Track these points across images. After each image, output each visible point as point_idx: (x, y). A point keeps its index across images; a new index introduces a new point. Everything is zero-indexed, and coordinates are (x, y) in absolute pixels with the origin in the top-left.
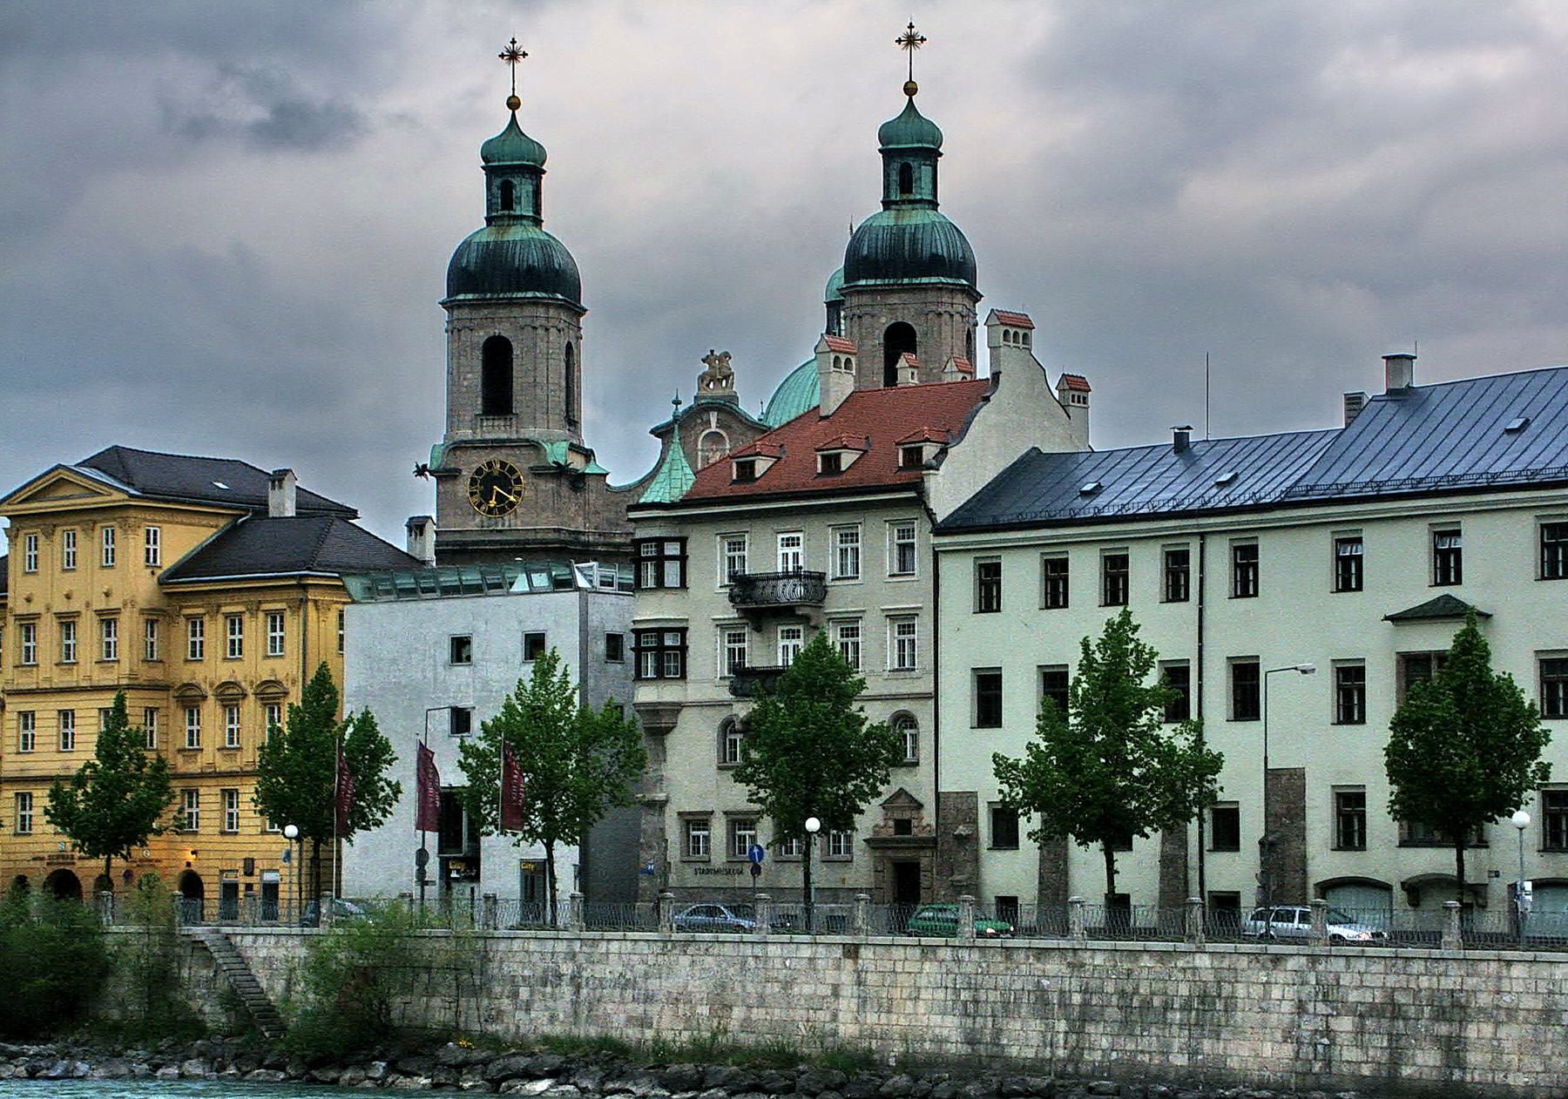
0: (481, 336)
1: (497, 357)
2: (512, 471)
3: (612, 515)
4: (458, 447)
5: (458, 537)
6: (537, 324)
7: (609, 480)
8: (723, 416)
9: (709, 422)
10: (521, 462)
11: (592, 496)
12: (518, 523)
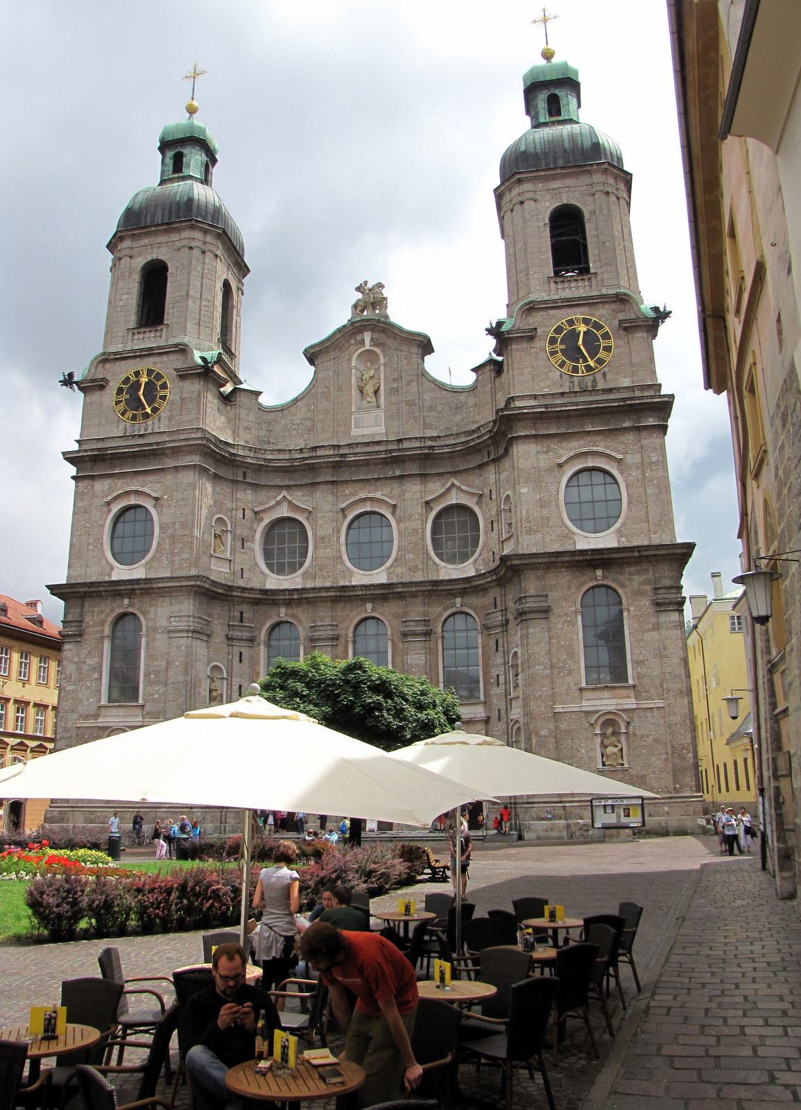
0: (140, 262)
1: (154, 280)
2: (159, 376)
3: (263, 433)
4: (106, 359)
5: (100, 445)
6: (193, 244)
7: (263, 400)
8: (376, 335)
9: (362, 342)
10: (167, 367)
11: (243, 412)
12: (161, 425)
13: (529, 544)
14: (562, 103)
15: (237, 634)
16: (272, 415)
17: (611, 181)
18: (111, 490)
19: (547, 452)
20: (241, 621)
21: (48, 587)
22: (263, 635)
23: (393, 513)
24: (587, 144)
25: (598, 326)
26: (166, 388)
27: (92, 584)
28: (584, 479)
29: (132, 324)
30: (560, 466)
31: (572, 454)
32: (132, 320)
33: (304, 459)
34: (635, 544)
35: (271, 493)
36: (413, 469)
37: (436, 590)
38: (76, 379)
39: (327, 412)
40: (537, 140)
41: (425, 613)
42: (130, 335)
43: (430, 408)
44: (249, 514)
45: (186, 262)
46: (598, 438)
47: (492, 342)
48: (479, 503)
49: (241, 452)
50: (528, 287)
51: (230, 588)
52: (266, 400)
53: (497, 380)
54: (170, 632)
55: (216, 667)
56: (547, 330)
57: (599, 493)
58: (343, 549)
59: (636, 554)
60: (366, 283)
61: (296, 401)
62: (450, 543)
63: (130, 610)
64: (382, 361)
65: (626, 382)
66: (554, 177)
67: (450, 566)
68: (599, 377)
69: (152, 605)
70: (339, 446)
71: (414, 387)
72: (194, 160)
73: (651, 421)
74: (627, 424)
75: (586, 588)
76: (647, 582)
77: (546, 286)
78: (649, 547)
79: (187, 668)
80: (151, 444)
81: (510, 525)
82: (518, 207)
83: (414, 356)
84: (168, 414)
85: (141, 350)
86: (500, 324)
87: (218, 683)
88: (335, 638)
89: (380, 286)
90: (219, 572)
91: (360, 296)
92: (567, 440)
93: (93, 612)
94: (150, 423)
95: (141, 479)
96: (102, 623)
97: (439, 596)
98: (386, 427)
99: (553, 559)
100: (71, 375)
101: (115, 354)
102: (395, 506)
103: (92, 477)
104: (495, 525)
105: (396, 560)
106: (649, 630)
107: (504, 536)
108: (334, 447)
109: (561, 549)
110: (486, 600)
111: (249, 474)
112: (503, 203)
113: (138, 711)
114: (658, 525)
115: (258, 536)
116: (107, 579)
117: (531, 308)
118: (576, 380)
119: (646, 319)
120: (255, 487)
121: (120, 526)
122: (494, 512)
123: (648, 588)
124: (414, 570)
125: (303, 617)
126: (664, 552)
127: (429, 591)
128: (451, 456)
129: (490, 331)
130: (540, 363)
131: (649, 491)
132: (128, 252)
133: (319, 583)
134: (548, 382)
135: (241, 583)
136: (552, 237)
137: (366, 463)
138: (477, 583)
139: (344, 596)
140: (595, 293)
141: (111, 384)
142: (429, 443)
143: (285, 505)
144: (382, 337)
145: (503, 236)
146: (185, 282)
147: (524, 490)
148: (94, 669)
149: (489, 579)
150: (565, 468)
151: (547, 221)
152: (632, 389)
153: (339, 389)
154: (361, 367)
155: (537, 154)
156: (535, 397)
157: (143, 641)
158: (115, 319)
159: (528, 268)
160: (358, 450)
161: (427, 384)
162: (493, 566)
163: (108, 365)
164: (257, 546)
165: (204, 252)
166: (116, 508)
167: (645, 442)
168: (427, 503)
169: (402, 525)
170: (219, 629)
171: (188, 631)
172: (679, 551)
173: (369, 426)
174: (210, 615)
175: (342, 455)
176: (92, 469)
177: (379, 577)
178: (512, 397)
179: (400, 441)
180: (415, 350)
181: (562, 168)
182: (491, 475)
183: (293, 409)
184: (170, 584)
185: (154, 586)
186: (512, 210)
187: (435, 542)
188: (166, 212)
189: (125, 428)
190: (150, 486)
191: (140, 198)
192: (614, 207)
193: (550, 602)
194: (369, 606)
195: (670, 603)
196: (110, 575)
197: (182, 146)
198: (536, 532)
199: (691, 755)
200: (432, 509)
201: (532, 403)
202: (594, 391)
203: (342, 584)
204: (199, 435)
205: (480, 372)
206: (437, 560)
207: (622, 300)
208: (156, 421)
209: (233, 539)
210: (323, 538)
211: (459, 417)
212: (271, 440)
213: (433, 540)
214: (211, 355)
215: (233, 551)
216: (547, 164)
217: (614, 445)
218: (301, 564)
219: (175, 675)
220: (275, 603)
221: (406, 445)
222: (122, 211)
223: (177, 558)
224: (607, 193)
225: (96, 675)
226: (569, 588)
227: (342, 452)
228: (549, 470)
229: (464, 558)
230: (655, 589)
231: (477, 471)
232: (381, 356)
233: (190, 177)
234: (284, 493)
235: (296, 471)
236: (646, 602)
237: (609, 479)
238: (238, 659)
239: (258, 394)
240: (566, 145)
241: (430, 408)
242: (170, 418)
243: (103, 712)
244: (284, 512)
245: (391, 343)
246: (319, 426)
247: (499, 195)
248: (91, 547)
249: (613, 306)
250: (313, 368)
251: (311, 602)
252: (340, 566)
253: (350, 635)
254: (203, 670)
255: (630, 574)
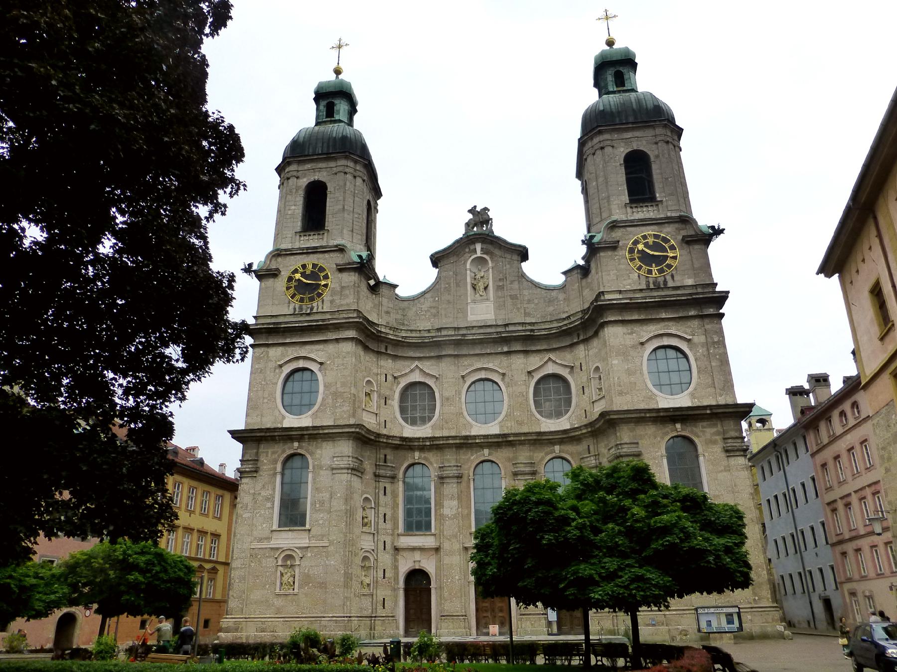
0: (304, 182)
2: (322, 269)
3: (399, 317)
4: (277, 254)
5: (273, 320)
6: (347, 170)
8: (485, 246)
9: (475, 251)
11: (385, 301)
12: (325, 306)
13: (621, 403)
14: (626, 77)
15: (382, 472)
16: (406, 303)
17: (669, 134)
18: (283, 355)
19: (631, 333)
20: (385, 462)
21: (229, 431)
22: (401, 475)
23: (503, 380)
24: (650, 105)
25: (666, 240)
26: (328, 278)
27: (268, 430)
28: (661, 353)
29: (299, 229)
30: (642, 344)
31: (652, 335)
32: (298, 225)
33: (433, 337)
34: (705, 403)
35: (407, 363)
36: (517, 347)
37: (540, 440)
38: (255, 267)
39: (449, 302)
40: (612, 103)
41: (531, 458)
42: (298, 237)
43: (529, 301)
44: (390, 378)
45: (341, 183)
46: (670, 324)
47: (583, 249)
48: (570, 373)
49: (383, 330)
50: (610, 210)
51: (379, 435)
52: (401, 292)
53: (584, 280)
54: (333, 469)
55: (366, 499)
56: (626, 242)
57: (673, 364)
58: (464, 406)
59: (708, 412)
60: (475, 207)
61: (424, 293)
62: (548, 404)
63: (299, 451)
64: (490, 264)
65: (690, 282)
66: (627, 130)
67: (548, 421)
68: (668, 278)
69: (317, 448)
70: (459, 328)
71: (516, 285)
72: (342, 107)
73: (711, 311)
74: (692, 313)
75: (669, 437)
76: (718, 433)
77: (624, 210)
78: (718, 406)
79: (348, 499)
80: (317, 321)
81: (600, 389)
82: (599, 152)
83: (516, 262)
84: (330, 298)
85: (308, 248)
86: (592, 237)
87: (368, 511)
88: (459, 477)
89: (486, 209)
90: (370, 422)
91: (471, 216)
92: (647, 324)
93: (267, 452)
94: (315, 304)
95: (308, 347)
96: (275, 462)
97: (542, 444)
98: (496, 315)
99: (643, 415)
100: (250, 265)
101: (286, 250)
102: (504, 375)
103: (267, 345)
104: (586, 390)
105: (506, 416)
106: (721, 471)
107: (594, 399)
108: (455, 328)
109: (647, 407)
110: (581, 448)
111: (390, 347)
112: (585, 149)
113: (306, 535)
114: (723, 389)
115: (397, 396)
116: (279, 426)
117: (614, 226)
118: (651, 280)
119: (704, 234)
120: (395, 357)
121: (289, 384)
122: (585, 379)
123: (718, 438)
124: (520, 423)
125: (433, 460)
126: (731, 410)
127: (535, 440)
128: (547, 338)
129: (583, 242)
130: (622, 267)
131: (713, 364)
132: (295, 174)
133: (446, 433)
134: (630, 281)
135: (384, 432)
136: (626, 174)
137: (481, 342)
138: (573, 434)
139: (466, 443)
140: (662, 216)
141: (282, 273)
142: (529, 328)
143: (417, 371)
144: (490, 247)
145: (580, 175)
146: (341, 198)
147: (615, 362)
148: (267, 499)
149: (584, 431)
150: (646, 346)
151: (622, 162)
152: (695, 286)
153: (458, 285)
154: (476, 270)
155: (612, 112)
156: (620, 292)
157: (310, 475)
158: (285, 225)
159: (609, 197)
160: (473, 331)
161: (525, 283)
162: (585, 421)
163: (279, 259)
164: (395, 403)
165: (355, 177)
166: (287, 369)
167: (708, 327)
168: (529, 373)
169: (510, 389)
170: (369, 467)
171: (348, 469)
172: (742, 410)
173: (482, 312)
174: (363, 457)
175: (464, 335)
176: (267, 339)
177: (493, 429)
178: (603, 293)
179: (506, 325)
180: (515, 257)
181: (633, 123)
182: (581, 350)
183: (422, 300)
184: (334, 431)
185: (321, 432)
186: (594, 154)
187: (537, 404)
188: (325, 145)
189: (295, 309)
190: (317, 353)
191: (303, 135)
192: (673, 153)
193: (641, 448)
194: (486, 451)
195: (738, 450)
196: (282, 423)
197: (333, 98)
198: (626, 394)
199: (765, 572)
200: (533, 377)
201: (618, 296)
202: (666, 287)
203: (464, 433)
204: (355, 315)
205: (569, 274)
206: (538, 416)
207: (686, 220)
208: (320, 303)
209: (379, 396)
210: (448, 399)
211: (551, 308)
212: (406, 323)
213: (535, 401)
214: (364, 254)
215: (379, 407)
216: (620, 120)
217: (684, 329)
218: (430, 419)
219: (338, 505)
220: (411, 449)
221: (511, 328)
222: (287, 141)
223: (338, 410)
224: (667, 142)
225: (269, 505)
226: (655, 437)
227: (461, 332)
228: (633, 347)
229: (559, 414)
230: (724, 439)
231: (568, 349)
232: (490, 262)
233: (340, 121)
234: (417, 363)
235: (426, 346)
236: (718, 449)
237: (680, 355)
238: (382, 492)
239: (395, 286)
240: (634, 106)
241: (529, 301)
242: (332, 302)
243: (275, 535)
244: (417, 377)
245: (497, 252)
246: (443, 312)
247: (582, 143)
248: (266, 401)
249: (677, 225)
250: (435, 271)
251: (441, 448)
252: (461, 420)
253: (471, 474)
254: (358, 501)
255: (703, 427)
